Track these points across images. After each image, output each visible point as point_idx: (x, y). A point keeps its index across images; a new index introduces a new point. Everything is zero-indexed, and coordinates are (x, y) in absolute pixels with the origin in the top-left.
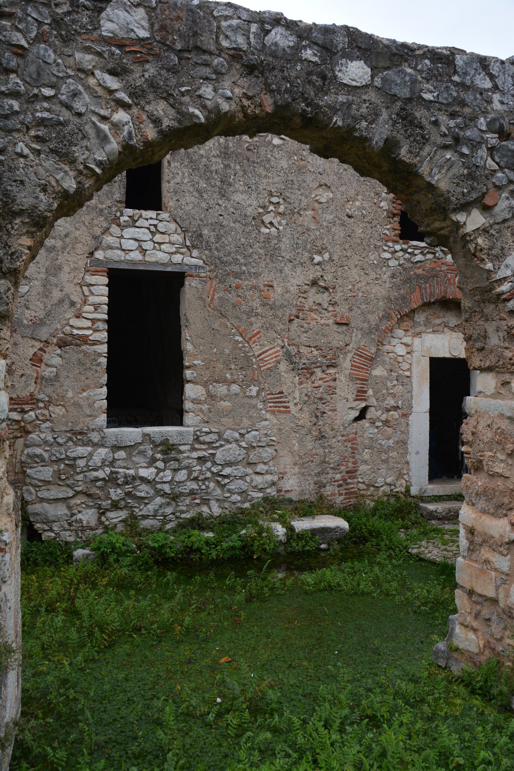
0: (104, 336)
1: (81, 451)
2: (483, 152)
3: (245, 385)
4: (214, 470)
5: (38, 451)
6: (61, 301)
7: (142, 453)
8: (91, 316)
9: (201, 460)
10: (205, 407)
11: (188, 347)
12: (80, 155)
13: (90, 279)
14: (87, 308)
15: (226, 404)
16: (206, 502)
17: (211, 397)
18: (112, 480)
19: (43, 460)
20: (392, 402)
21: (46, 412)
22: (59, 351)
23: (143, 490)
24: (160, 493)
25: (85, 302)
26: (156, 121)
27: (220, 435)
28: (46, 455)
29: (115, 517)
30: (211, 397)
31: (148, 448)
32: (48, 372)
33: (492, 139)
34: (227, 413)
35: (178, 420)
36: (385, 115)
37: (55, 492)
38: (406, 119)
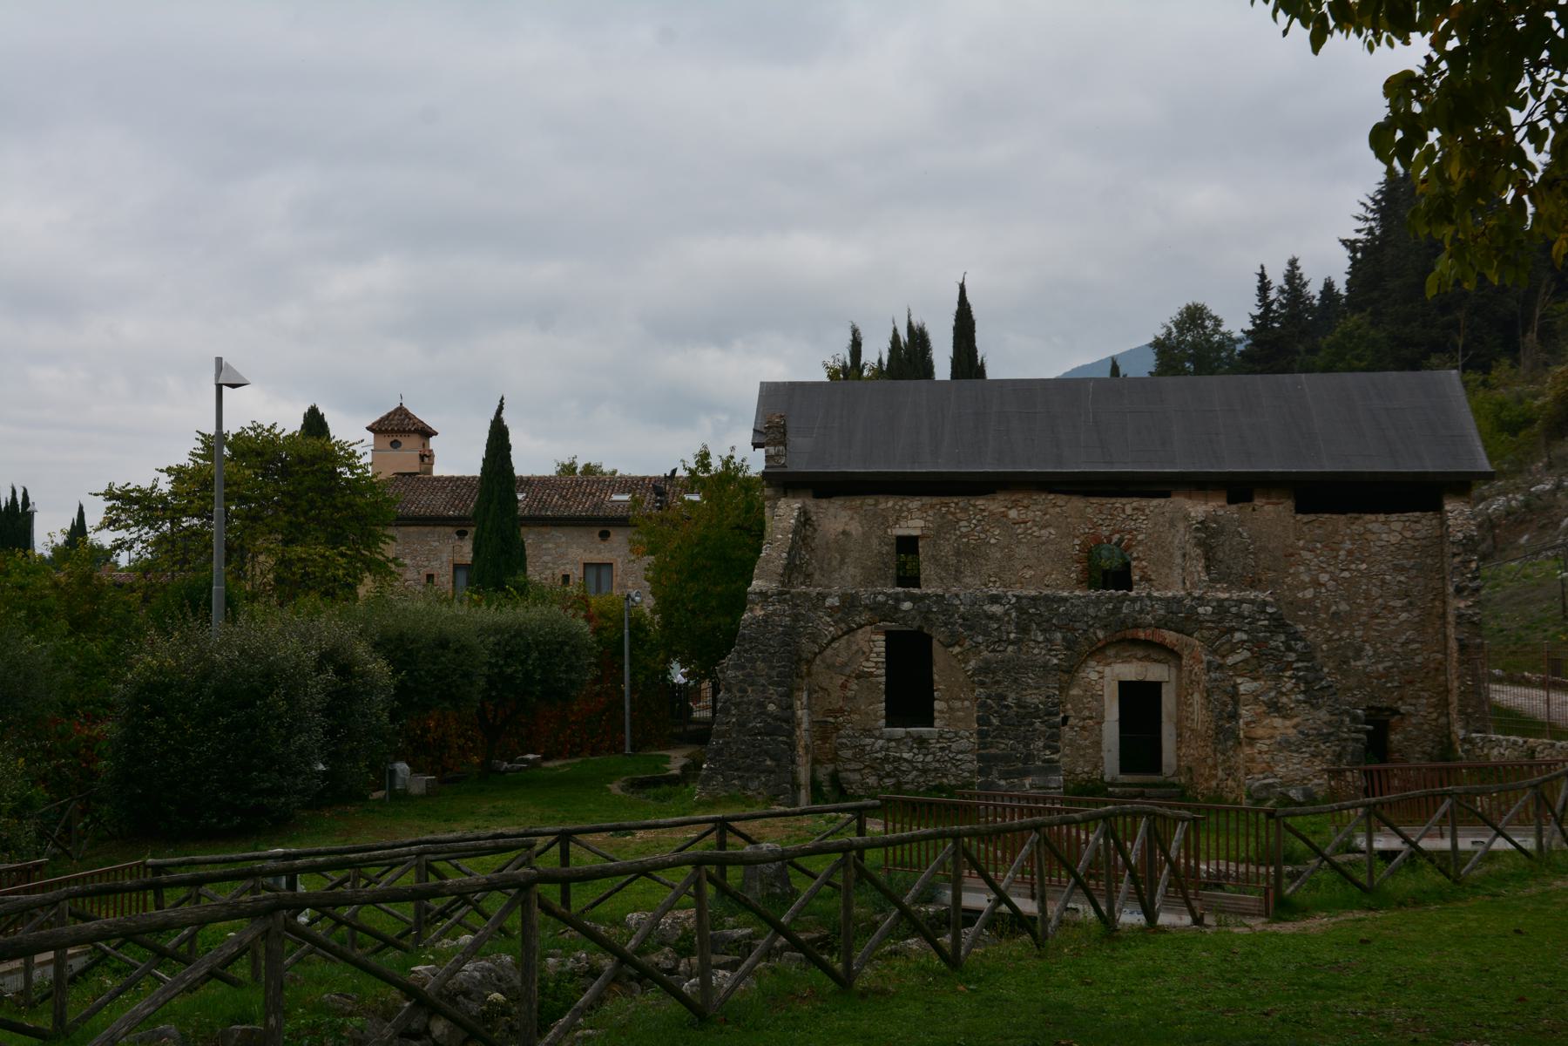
1: (868, 741)
9: (942, 749)
11: (936, 677)
17: (950, 708)
18: (886, 759)
20: (1087, 713)
23: (905, 766)
24: (915, 768)
27: (956, 734)
29: (888, 782)
30: (950, 708)
31: (909, 740)
32: (850, 694)
35: (932, 726)
37: (854, 766)
38: (926, 619)
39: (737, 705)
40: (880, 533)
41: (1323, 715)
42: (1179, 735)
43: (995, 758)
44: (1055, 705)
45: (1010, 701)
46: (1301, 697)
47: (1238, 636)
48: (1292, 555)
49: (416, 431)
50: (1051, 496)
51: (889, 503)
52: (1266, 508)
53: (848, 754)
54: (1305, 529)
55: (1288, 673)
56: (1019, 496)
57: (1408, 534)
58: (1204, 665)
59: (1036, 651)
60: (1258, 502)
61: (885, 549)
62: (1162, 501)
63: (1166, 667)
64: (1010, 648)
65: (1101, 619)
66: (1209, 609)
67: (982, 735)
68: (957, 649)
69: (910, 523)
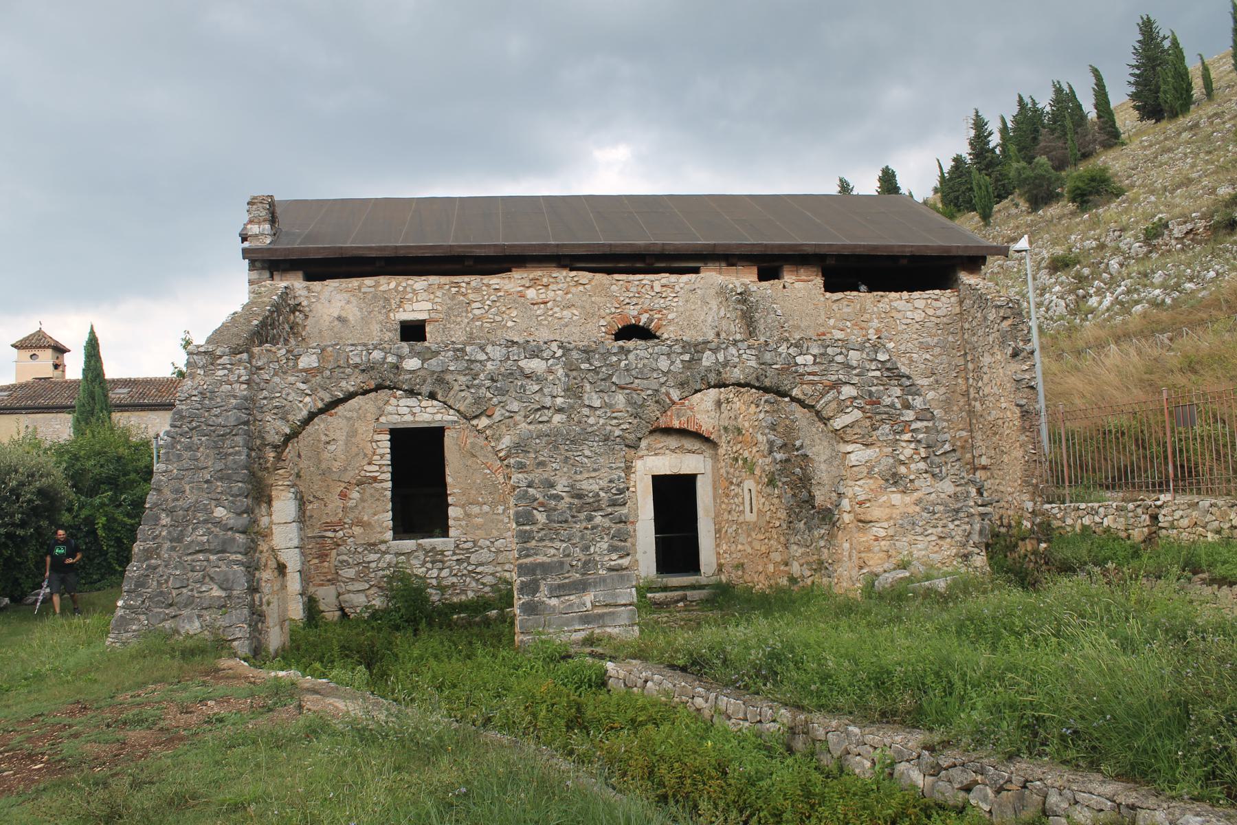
0: (388, 476)
1: (373, 557)
2: (483, 390)
3: (493, 505)
4: (470, 568)
5: (345, 558)
7: (416, 557)
10: (463, 523)
11: (449, 480)
12: (290, 417)
13: (377, 437)
14: (375, 457)
15: (480, 520)
16: (464, 592)
17: (468, 515)
25: (374, 454)
26: (322, 400)
30: (468, 515)
31: (421, 554)
32: (351, 503)
33: (488, 383)
34: (479, 527)
35: (445, 534)
36: (429, 380)
39: (171, 512)
40: (381, 317)
41: (947, 487)
42: (718, 531)
43: (546, 568)
44: (621, 492)
45: (559, 489)
46: (922, 465)
47: (848, 391)
48: (824, 334)
49: (49, 347)
50: (574, 273)
51: (388, 284)
52: (798, 285)
53: (350, 573)
54: (835, 307)
55: (907, 436)
56: (540, 273)
57: (930, 312)
58: (764, 447)
59: (591, 421)
60: (788, 278)
61: (388, 336)
62: (693, 276)
63: (701, 457)
64: (557, 418)
65: (675, 375)
66: (810, 359)
67: (524, 537)
68: (483, 422)
69: (416, 306)
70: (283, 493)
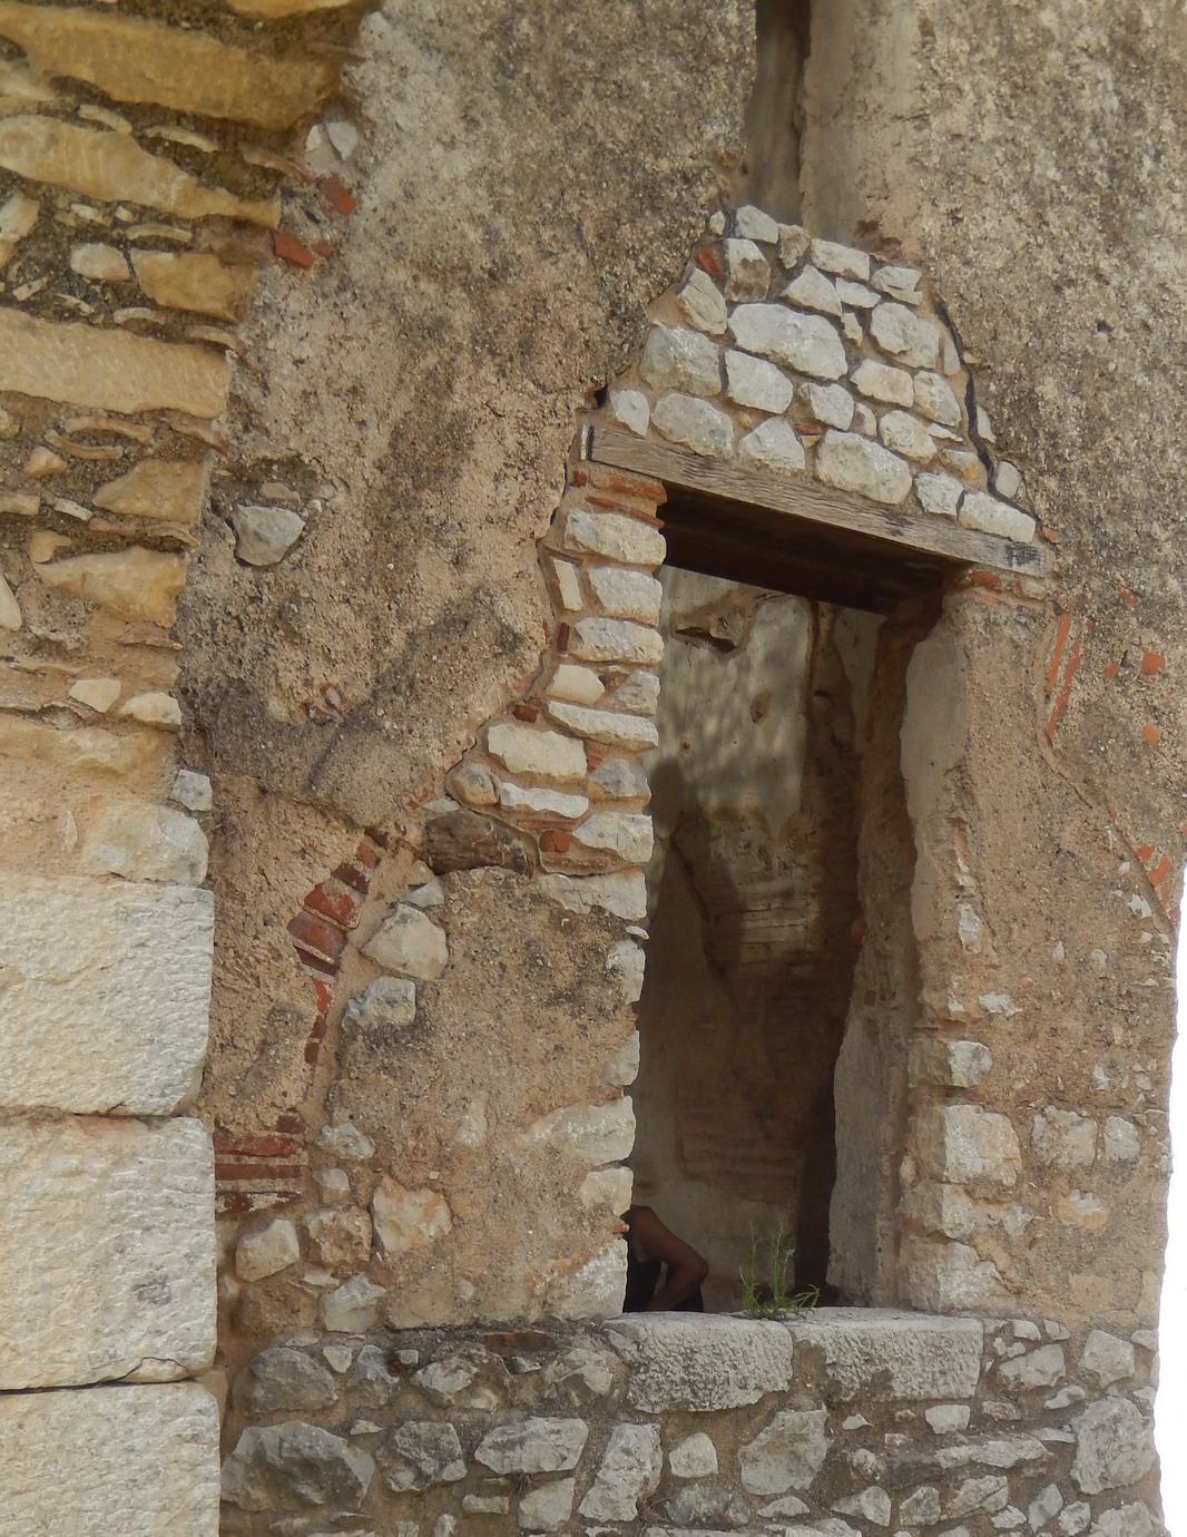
5: (319, 1441)
6: (455, 622)
8: (589, 721)
10: (1015, 1219)
13: (585, 526)
17: (1040, 1170)
19: (342, 1488)
21: (357, 1224)
22: (432, 892)
28: (361, 1465)
30: (1040, 1170)
70: (121, 809)
